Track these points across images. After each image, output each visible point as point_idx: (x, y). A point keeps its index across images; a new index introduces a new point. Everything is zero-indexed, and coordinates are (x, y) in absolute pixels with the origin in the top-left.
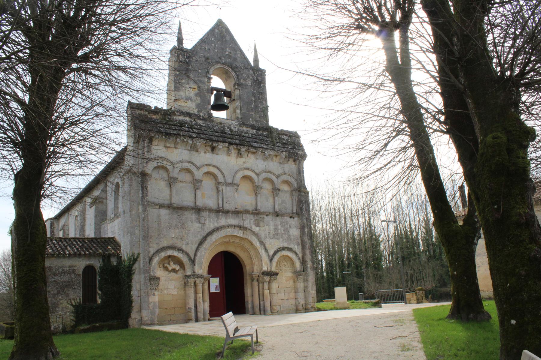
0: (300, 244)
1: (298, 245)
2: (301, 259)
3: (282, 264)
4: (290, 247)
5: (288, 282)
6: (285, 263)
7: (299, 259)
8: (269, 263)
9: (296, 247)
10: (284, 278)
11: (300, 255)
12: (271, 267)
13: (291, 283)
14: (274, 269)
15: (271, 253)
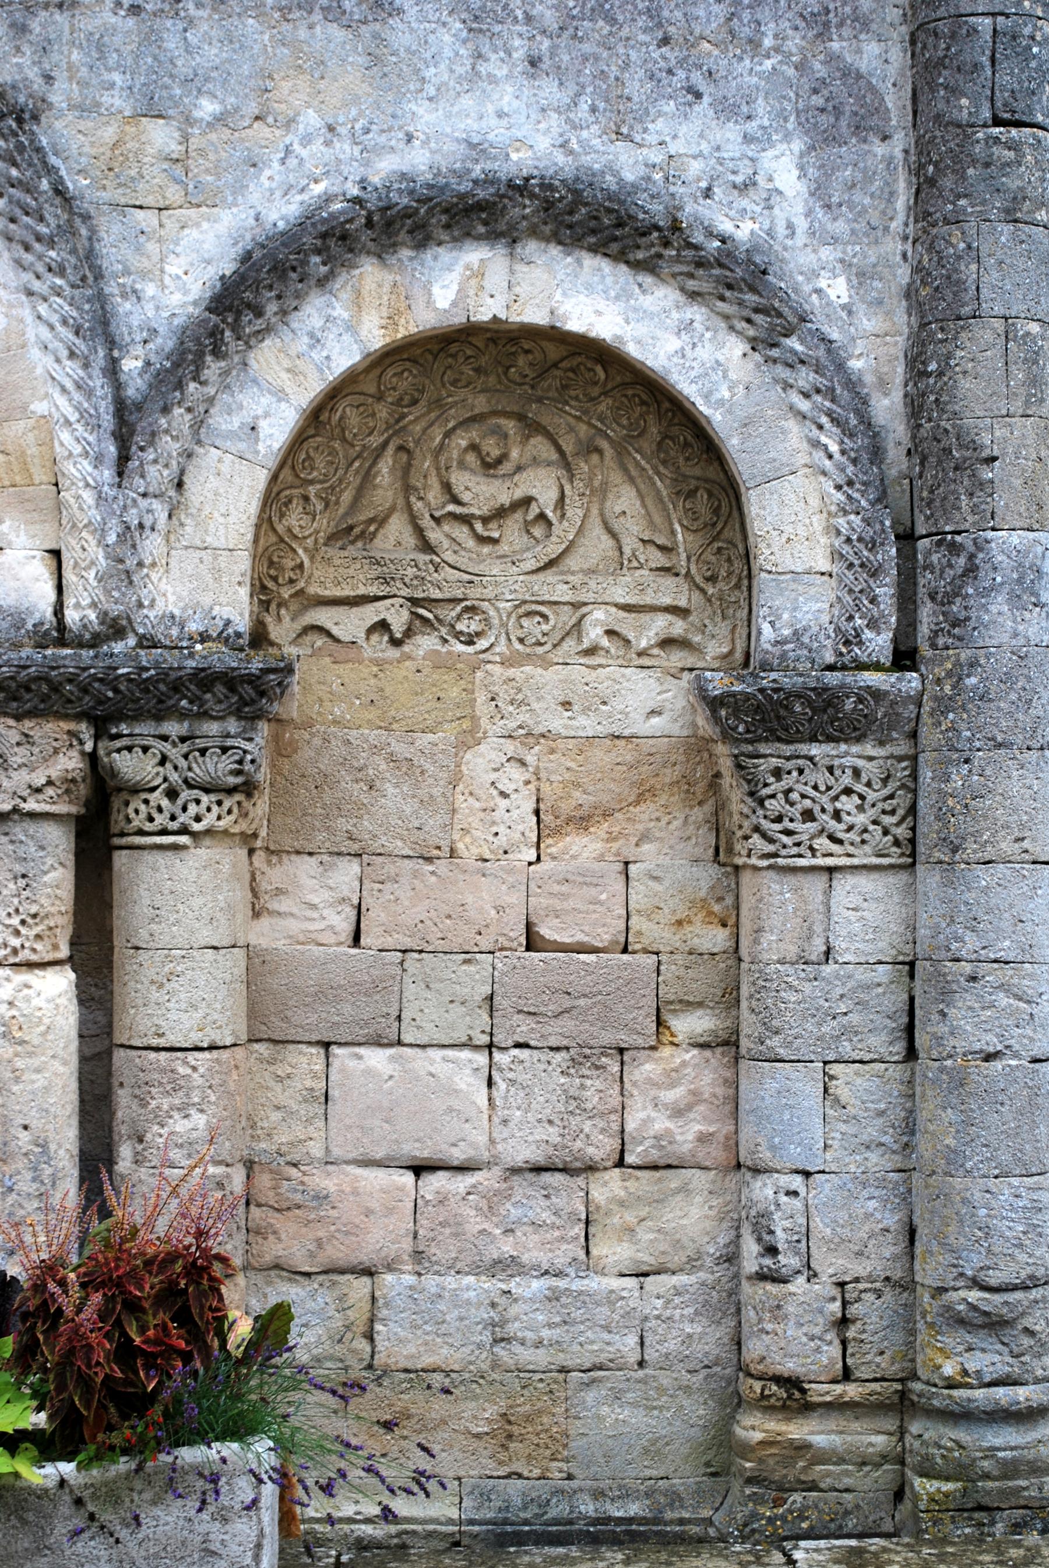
0: (895, 102)
1: (835, 116)
2: (888, 408)
3: (480, 492)
4: (626, 164)
5: (583, 848)
6: (542, 486)
7: (843, 401)
8: (84, 473)
9: (784, 168)
10: (483, 761)
11: (873, 344)
12: (124, 571)
13: (668, 861)
14: (197, 584)
15: (173, 275)
